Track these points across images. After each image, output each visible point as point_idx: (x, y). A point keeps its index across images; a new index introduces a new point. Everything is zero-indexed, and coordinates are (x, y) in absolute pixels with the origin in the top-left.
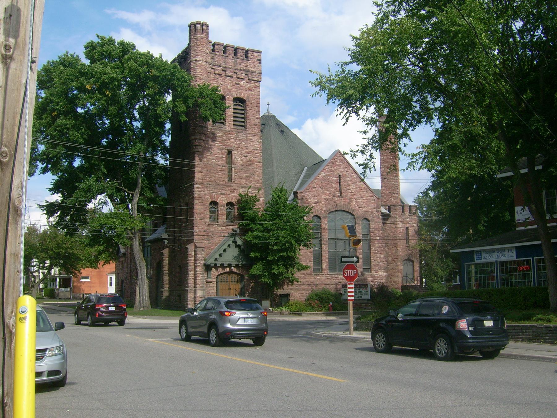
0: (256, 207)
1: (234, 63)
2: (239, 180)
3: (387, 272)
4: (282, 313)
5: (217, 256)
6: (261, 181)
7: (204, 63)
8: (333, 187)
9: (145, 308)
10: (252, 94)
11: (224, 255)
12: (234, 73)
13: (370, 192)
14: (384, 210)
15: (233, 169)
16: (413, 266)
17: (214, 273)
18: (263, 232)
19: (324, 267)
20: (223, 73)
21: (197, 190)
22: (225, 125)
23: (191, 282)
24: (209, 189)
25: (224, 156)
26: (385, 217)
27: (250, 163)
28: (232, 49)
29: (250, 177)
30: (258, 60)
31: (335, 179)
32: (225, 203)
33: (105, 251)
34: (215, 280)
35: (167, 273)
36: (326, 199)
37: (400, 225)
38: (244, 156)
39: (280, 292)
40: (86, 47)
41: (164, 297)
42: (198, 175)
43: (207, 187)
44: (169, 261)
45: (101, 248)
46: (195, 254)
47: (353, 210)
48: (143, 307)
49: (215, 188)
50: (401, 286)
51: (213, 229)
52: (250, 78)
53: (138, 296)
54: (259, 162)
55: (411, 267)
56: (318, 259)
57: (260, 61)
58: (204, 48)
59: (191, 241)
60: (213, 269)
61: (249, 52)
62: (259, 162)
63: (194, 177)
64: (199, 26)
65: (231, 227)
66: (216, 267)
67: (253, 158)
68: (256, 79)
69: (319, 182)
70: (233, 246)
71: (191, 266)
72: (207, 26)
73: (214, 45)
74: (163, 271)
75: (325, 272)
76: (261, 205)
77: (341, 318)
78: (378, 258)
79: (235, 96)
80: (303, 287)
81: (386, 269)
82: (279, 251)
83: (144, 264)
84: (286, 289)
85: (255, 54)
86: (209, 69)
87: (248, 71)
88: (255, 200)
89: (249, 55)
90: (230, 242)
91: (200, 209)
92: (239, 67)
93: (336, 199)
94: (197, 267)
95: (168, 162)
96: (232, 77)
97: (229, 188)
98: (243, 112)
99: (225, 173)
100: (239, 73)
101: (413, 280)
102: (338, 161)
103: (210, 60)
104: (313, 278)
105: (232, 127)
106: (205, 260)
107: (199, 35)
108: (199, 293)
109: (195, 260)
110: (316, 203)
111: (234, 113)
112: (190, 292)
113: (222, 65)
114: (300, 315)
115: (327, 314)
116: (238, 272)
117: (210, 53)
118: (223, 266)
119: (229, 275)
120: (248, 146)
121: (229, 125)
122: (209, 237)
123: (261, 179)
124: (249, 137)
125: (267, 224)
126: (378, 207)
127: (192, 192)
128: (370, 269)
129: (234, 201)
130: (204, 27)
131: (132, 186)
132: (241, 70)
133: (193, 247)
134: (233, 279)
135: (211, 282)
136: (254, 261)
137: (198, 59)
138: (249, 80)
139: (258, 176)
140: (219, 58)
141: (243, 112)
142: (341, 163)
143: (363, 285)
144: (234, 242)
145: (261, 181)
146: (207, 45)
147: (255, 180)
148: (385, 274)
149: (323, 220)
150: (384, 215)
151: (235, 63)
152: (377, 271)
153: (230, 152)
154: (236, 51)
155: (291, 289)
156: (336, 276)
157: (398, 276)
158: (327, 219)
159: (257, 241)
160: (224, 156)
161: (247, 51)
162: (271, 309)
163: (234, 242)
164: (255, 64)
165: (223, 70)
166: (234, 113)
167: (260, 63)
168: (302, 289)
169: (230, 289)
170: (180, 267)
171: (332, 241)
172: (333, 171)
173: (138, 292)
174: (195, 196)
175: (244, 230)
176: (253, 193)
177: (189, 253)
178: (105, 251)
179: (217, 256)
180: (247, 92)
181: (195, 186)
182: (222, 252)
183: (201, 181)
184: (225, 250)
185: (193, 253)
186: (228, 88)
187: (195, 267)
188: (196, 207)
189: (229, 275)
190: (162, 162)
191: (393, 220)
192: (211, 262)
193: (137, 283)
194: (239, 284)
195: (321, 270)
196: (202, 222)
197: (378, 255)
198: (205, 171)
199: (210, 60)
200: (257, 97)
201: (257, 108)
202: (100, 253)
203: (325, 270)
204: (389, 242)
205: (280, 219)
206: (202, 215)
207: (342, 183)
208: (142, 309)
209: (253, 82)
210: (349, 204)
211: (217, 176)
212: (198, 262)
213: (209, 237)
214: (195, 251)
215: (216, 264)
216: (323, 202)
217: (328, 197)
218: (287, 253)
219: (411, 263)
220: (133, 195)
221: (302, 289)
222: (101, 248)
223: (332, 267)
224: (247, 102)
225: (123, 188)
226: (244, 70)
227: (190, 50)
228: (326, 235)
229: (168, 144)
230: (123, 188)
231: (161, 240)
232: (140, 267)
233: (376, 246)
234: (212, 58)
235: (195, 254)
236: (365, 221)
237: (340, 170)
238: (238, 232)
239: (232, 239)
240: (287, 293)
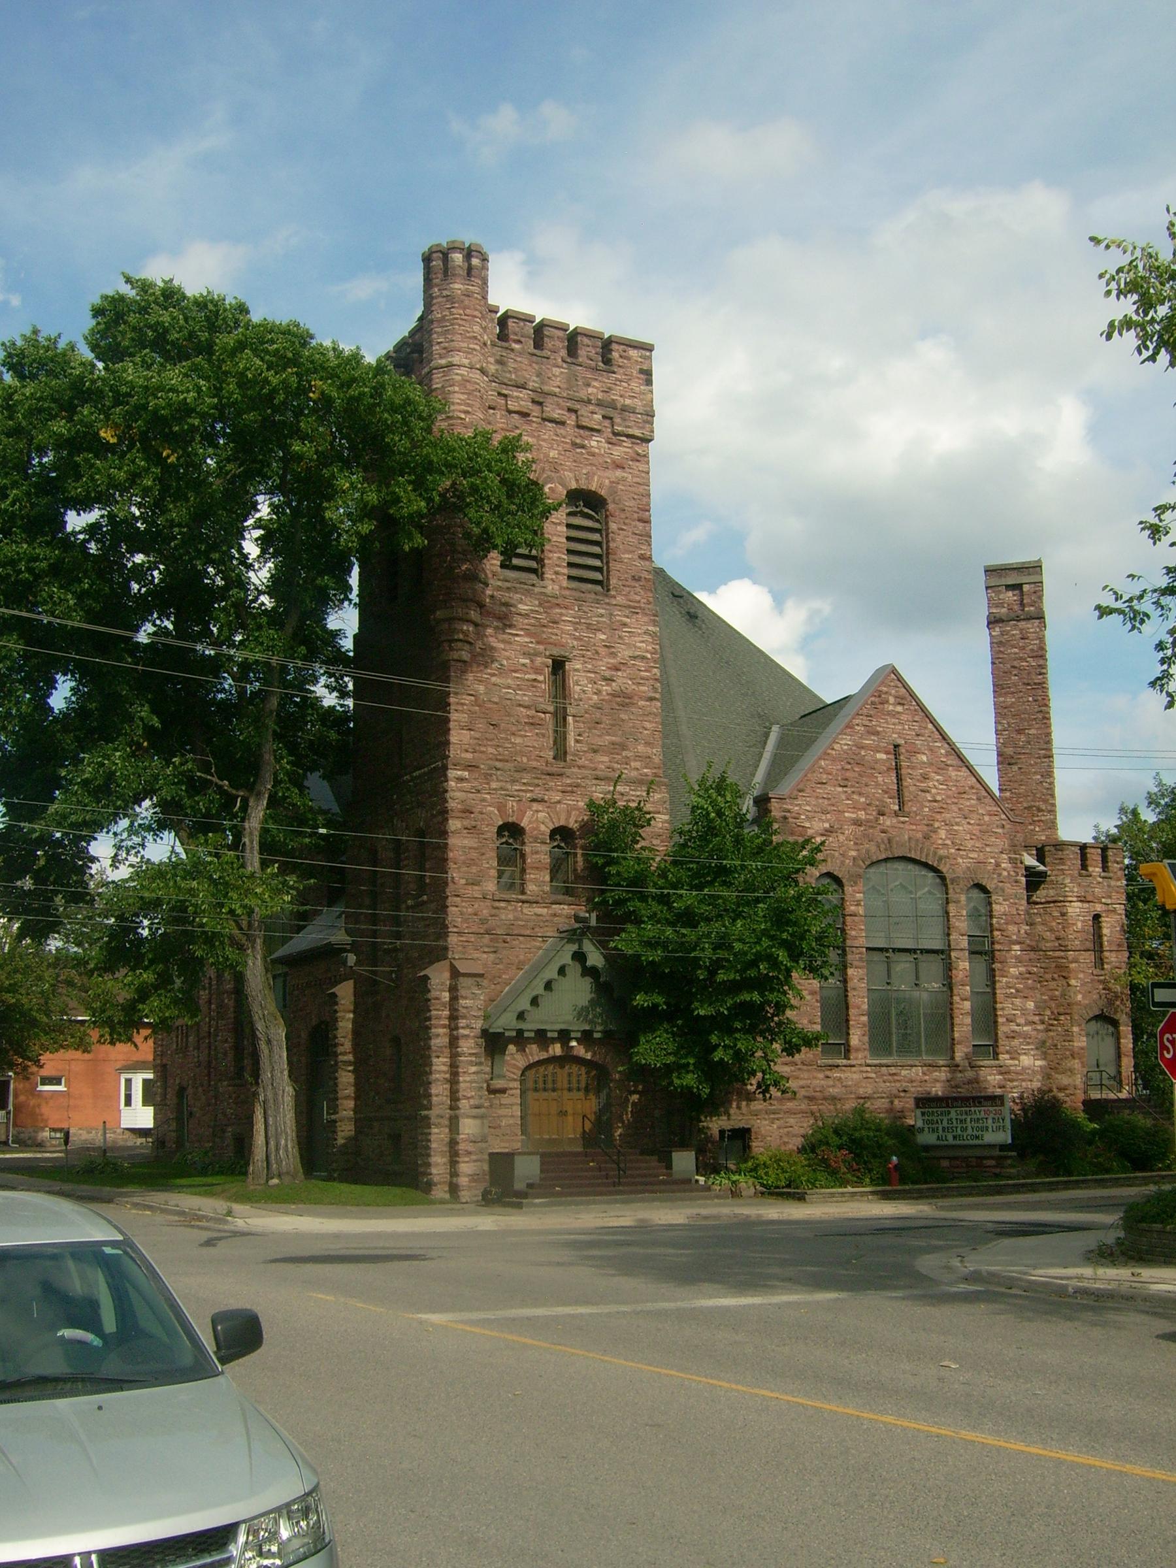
0: (642, 843)
1: (568, 381)
2: (590, 755)
3: (1044, 1056)
4: (735, 1193)
5: (524, 1004)
6: (656, 760)
7: (476, 376)
8: (877, 785)
9: (287, 1179)
10: (624, 479)
11: (547, 1001)
12: (570, 410)
13: (988, 800)
14: (1030, 861)
15: (570, 719)
16: (1117, 1037)
17: (515, 1059)
18: (672, 924)
19: (854, 1041)
20: (535, 411)
21: (458, 787)
22: (541, 577)
23: (439, 1091)
24: (494, 785)
25: (541, 678)
26: (1034, 880)
27: (624, 699)
28: (560, 333)
29: (624, 747)
30: (642, 371)
31: (881, 756)
32: (546, 829)
33: (156, 987)
34: (517, 1084)
35: (349, 1063)
36: (857, 823)
37: (1075, 909)
38: (605, 679)
39: (715, 1125)
40: (98, 312)
41: (340, 1141)
42: (458, 738)
43: (487, 777)
44: (354, 1022)
45: (148, 977)
46: (454, 999)
47: (941, 859)
48: (280, 1176)
49: (513, 781)
50: (1084, 1103)
51: (508, 914)
52: (618, 428)
53: (259, 1139)
54: (651, 699)
55: (1110, 1041)
56: (837, 1013)
57: (647, 375)
58: (476, 328)
59: (439, 954)
60: (512, 1048)
61: (614, 346)
62: (651, 699)
63: (447, 743)
64: (458, 258)
65: (566, 910)
66: (520, 1039)
67: (631, 686)
68: (637, 432)
69: (835, 768)
70: (575, 970)
71: (439, 1038)
72: (485, 260)
73: (503, 321)
74: (336, 1055)
75: (857, 1058)
76: (659, 836)
77: (942, 1208)
78: (1018, 1010)
79: (574, 486)
80: (790, 1105)
81: (1043, 1048)
82: (734, 987)
83: (280, 1033)
84: (737, 1116)
85: (633, 353)
86: (492, 396)
87: (612, 405)
88: (636, 819)
89: (615, 355)
90: (566, 958)
91: (468, 850)
92: (583, 394)
93: (888, 823)
94: (462, 1043)
95: (350, 703)
96: (563, 423)
97: (558, 783)
98: (596, 537)
99: (530, 740)
100: (584, 411)
101: (1118, 1079)
102: (892, 700)
103: (492, 368)
104: (821, 1076)
105: (565, 583)
106: (486, 1018)
107: (458, 286)
108: (469, 1127)
109: (453, 1017)
110: (828, 832)
111: (569, 539)
112: (437, 1125)
113: (531, 385)
114: (801, 1198)
115: (886, 1196)
116: (589, 1056)
117: (494, 345)
118: (541, 1037)
119: (562, 1067)
120: (614, 650)
121: (556, 578)
122: (498, 938)
123: (656, 754)
124: (620, 616)
125: (687, 898)
126: (1014, 848)
127: (440, 793)
128: (995, 1046)
129: (573, 825)
130: (475, 261)
131: (243, 770)
132: (589, 402)
133: (447, 975)
134: (574, 1079)
135: (503, 1091)
136: (649, 1019)
137: (456, 360)
138: (615, 434)
139: (647, 744)
140: (521, 364)
141: (596, 537)
142: (899, 709)
143: (974, 1098)
144: (579, 957)
145: (656, 760)
146: (483, 317)
147: (638, 757)
148: (1038, 1063)
149: (848, 889)
150: (1030, 872)
151: (571, 379)
153: (558, 666)
154: (574, 339)
155: (756, 1114)
156: (893, 1070)
157: (1071, 1070)
158: (861, 886)
159: (656, 955)
160: (541, 678)
161: (607, 345)
162: (702, 1179)
163: (579, 957)
164: (634, 384)
165: (533, 402)
166: (569, 539)
167: (649, 382)
168: (790, 1112)
169: (562, 1113)
170: (396, 1041)
171: (877, 956)
172: (877, 733)
173: (259, 1127)
174: (452, 804)
175: (613, 919)
176: (628, 795)
177: (433, 994)
178: (156, 987)
179: (524, 1004)
180: (609, 473)
181: (452, 774)
182: (540, 990)
183: (469, 756)
184: (548, 986)
185: (446, 996)
186: (556, 461)
187: (454, 1041)
188: (452, 841)
189: (562, 1067)
190: (330, 700)
191: (1052, 893)
192: (506, 1022)
193: (255, 1094)
194: (592, 1096)
195: (847, 1051)
196: (476, 891)
197: (1018, 1001)
198: (481, 725)
199: (492, 368)
200: (641, 489)
201: (640, 525)
202: (143, 994)
203: (857, 1050)
204: (1050, 964)
205: (724, 883)
206: (474, 869)
207: (903, 771)
208: (275, 1181)
209: (627, 443)
210: (927, 837)
211: (518, 740)
212: (462, 1022)
213: (498, 938)
214: (453, 989)
215: (520, 1032)
216: (849, 830)
217: (862, 815)
218: (762, 995)
219: (1111, 1029)
220: (245, 802)
221: (790, 1112)
222: (148, 977)
223: (880, 1042)
224: (611, 507)
225: (215, 779)
226: (600, 404)
227: (430, 332)
228: (859, 936)
229: (347, 644)
230: (215, 779)
231: (329, 953)
232: (269, 1042)
233: (1012, 973)
234: (500, 362)
235: (454, 999)
236: (976, 894)
237: (896, 729)
238: (593, 922)
239: (575, 947)
240: (741, 1125)
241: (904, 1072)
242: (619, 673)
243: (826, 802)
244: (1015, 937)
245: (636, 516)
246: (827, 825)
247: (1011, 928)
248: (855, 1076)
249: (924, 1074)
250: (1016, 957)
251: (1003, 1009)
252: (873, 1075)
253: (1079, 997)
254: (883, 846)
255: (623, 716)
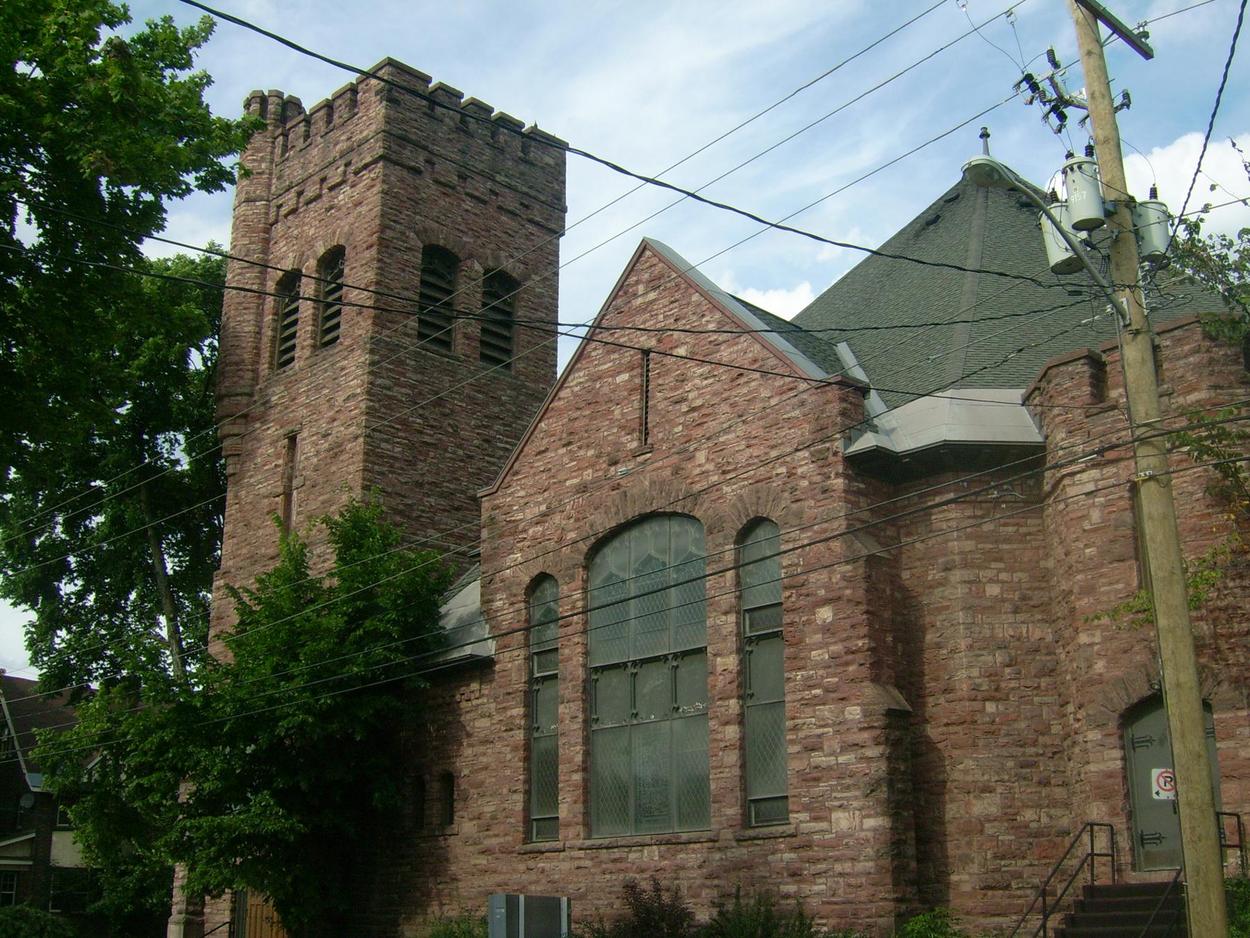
19: (563, 812)
36: (583, 489)
68: (368, 159)
75: (572, 835)
104: (522, 867)
148: (870, 823)
152: (819, 812)
156: (616, 853)
197: (826, 711)
211: (261, 532)
217: (588, 475)
241: (632, 856)
242: (335, 424)
243: (544, 476)
244: (822, 592)
245: (365, 246)
246: (543, 508)
247: (813, 577)
248: (565, 866)
249: (662, 857)
250: (827, 629)
251: (795, 728)
252: (588, 863)
253: (1100, 666)
254: (613, 510)
255: (334, 468)
